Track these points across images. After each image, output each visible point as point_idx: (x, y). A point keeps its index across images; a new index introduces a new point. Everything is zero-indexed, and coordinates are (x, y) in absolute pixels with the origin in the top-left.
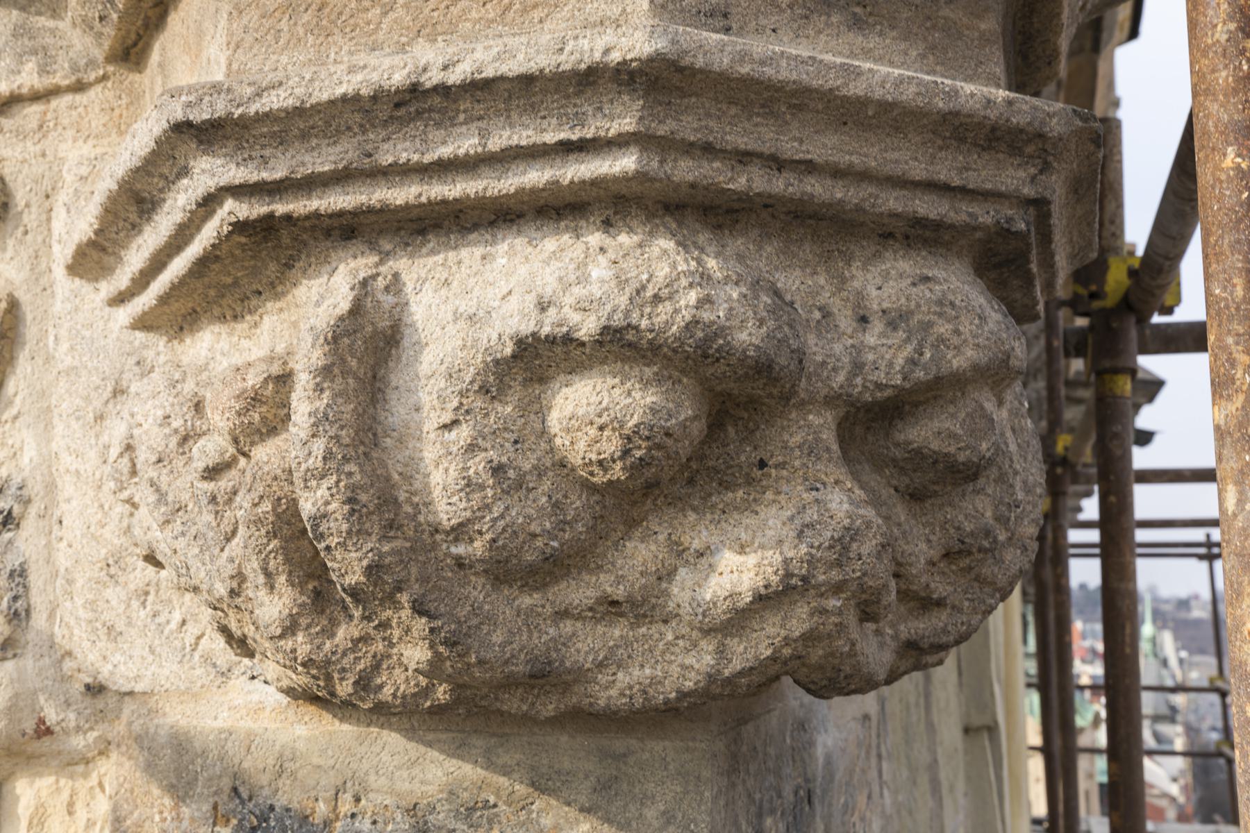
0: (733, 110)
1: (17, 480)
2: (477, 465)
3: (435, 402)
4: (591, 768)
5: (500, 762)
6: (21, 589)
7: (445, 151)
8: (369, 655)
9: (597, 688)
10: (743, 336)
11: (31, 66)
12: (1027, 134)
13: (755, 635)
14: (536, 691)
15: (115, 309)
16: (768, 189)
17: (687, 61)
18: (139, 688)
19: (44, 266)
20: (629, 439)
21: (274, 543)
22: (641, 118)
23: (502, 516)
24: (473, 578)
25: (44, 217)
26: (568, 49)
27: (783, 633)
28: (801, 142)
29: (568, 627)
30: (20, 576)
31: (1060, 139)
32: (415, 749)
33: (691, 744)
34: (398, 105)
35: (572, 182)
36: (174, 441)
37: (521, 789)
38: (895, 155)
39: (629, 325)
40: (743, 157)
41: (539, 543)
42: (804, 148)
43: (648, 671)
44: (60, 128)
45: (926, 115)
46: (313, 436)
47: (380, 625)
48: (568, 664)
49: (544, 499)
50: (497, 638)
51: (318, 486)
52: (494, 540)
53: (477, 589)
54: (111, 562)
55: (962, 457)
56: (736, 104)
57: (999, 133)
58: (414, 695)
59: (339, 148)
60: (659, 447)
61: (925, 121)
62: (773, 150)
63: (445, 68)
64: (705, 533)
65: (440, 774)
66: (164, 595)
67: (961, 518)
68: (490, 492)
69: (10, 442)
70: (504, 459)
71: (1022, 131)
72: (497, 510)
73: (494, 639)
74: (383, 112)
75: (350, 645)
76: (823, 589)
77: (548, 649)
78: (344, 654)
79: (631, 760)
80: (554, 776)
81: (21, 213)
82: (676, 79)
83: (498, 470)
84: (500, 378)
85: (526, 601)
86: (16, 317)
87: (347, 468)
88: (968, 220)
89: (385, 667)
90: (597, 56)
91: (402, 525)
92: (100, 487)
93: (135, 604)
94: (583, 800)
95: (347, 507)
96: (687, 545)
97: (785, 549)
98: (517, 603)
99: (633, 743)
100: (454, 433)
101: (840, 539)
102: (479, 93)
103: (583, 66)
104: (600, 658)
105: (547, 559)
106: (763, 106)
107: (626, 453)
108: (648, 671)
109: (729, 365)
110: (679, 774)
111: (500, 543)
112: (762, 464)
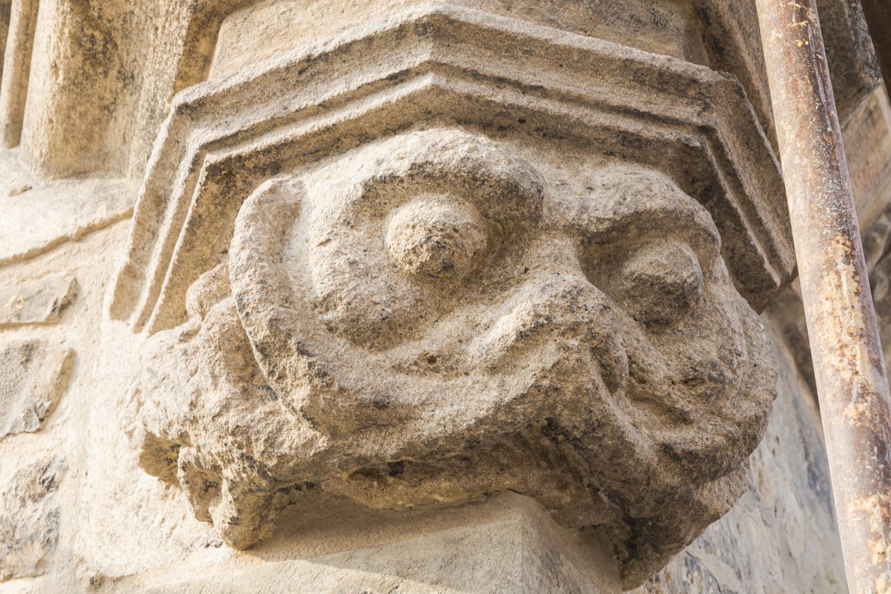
0: (489, 53)
1: (61, 457)
2: (341, 262)
3: (318, 233)
4: (439, 553)
5: (375, 564)
6: (54, 525)
7: (326, 96)
8: (275, 422)
9: (422, 422)
10: (499, 168)
11: (103, 207)
12: (685, 79)
13: (523, 371)
14: (383, 434)
15: (138, 334)
16: (516, 102)
17: (454, 17)
18: (127, 572)
19: (95, 327)
20: (430, 230)
21: (220, 354)
22: (432, 53)
23: (354, 289)
24: (338, 339)
25: (100, 297)
26: (390, 20)
27: (541, 365)
28: (535, 76)
29: (401, 378)
30: (55, 516)
31: (710, 85)
32: (316, 568)
33: (508, 522)
34: (300, 73)
35: (397, 101)
36: (165, 348)
37: (390, 579)
38: (599, 89)
39: (427, 162)
40: (500, 82)
41: (379, 308)
42: (537, 78)
43: (455, 407)
44: (116, 242)
45: (612, 61)
46: (242, 248)
47: (279, 378)
48: (401, 400)
49: (383, 283)
50: (353, 375)
51: (243, 278)
52: (349, 304)
53: (341, 345)
54: (118, 491)
55: (669, 280)
56: (490, 49)
57: (665, 78)
58: (304, 446)
59: (269, 108)
60: (450, 237)
61: (613, 67)
62: (516, 78)
63: (325, 44)
64: (490, 314)
65: (333, 581)
66: (151, 506)
67: (691, 351)
68: (347, 276)
69: (59, 436)
70: (357, 259)
71: (680, 76)
72: (352, 285)
73: (351, 376)
74: (293, 77)
75: (263, 416)
76: (563, 328)
77: (388, 388)
78: (259, 421)
79: (466, 542)
80: (413, 565)
81: (85, 299)
82: (450, 28)
83: (353, 263)
84: (357, 213)
85: (373, 358)
86: (73, 362)
87: (261, 264)
88: (657, 136)
89: (285, 429)
90: (405, 18)
91: (293, 302)
92: (116, 445)
93: (132, 513)
94: (433, 576)
95: (259, 286)
96: (478, 321)
97: (534, 299)
98: (367, 358)
99: (468, 529)
100: (327, 248)
101: (569, 292)
102: (344, 55)
103: (398, 25)
104: (424, 399)
105: (384, 319)
106: (507, 51)
107: (428, 239)
108: (455, 407)
109: (491, 186)
110: (500, 543)
111: (353, 305)
112: (526, 270)
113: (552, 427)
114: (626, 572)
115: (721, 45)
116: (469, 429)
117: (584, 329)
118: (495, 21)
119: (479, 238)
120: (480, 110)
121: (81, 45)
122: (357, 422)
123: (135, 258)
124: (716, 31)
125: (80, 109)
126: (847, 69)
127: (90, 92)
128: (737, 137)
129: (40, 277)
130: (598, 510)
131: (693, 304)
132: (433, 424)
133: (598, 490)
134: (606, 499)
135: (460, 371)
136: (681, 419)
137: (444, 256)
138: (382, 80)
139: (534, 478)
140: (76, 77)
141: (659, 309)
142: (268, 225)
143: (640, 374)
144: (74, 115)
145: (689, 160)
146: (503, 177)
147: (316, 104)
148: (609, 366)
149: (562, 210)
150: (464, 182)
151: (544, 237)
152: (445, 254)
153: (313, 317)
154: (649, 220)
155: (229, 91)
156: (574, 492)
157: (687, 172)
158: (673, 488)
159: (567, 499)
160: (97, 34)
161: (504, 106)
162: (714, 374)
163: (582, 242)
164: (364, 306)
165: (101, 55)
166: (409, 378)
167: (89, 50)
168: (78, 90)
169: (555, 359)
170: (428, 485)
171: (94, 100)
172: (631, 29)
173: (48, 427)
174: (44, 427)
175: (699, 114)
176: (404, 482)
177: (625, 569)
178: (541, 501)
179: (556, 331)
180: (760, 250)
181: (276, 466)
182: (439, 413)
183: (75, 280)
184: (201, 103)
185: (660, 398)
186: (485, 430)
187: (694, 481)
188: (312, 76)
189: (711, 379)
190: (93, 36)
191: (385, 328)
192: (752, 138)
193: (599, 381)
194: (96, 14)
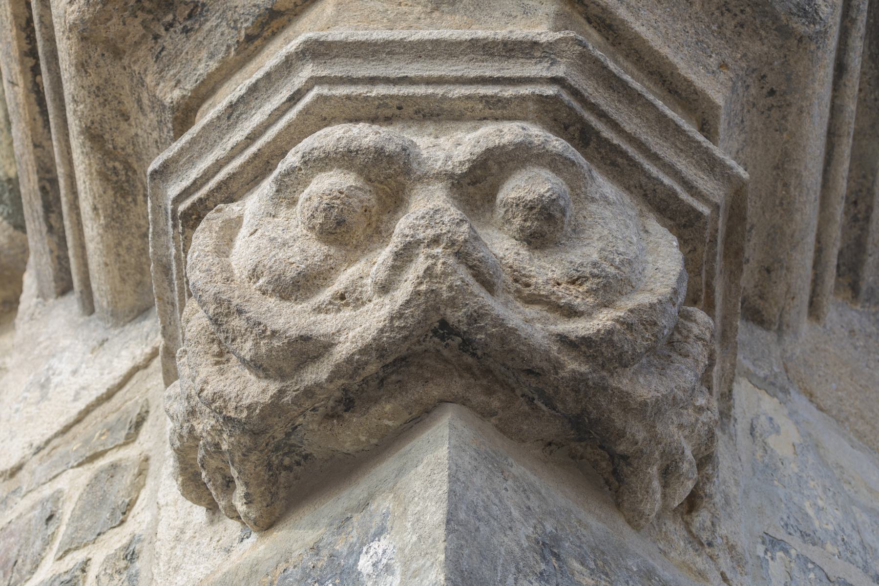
0: (359, 61)
23: (274, 256)
34: (229, 118)
40: (373, 81)
50: (282, 321)
71: (521, 42)
74: (224, 123)
82: (322, 49)
113: (444, 329)
114: (620, 500)
115: (608, 22)
116: (374, 340)
118: (358, 35)
119: (371, 200)
120: (363, 107)
121: (108, 180)
122: (294, 359)
123: (167, 337)
124: (596, 11)
125: (125, 243)
126: (773, 23)
127: (128, 224)
128: (597, 83)
129: (120, 408)
130: (538, 417)
131: (558, 215)
132: (348, 344)
133: (534, 399)
134: (544, 407)
135: (364, 299)
136: (571, 312)
137: (335, 214)
138: (284, 103)
139: (457, 386)
140: (113, 212)
141: (528, 224)
142: (214, 234)
143: (524, 279)
144: (122, 252)
145: (550, 109)
146: (371, 144)
147: (243, 138)
148: (475, 266)
149: (430, 162)
150: (343, 156)
151: (419, 186)
152: (335, 212)
153: (249, 287)
155: (182, 149)
156: (503, 398)
157: (555, 120)
158: (581, 374)
159: (495, 404)
160: (117, 164)
161: (379, 98)
162: (595, 271)
163: (453, 184)
164: (282, 267)
165: (126, 184)
166: (328, 317)
167: (116, 182)
168: (118, 225)
169: (425, 266)
170: (373, 410)
171: (133, 230)
172: (503, 23)
173: (129, 518)
174: (126, 518)
175: (548, 68)
176: (357, 415)
177: (618, 497)
178: (472, 408)
179: (422, 245)
180: (667, 181)
181: (248, 417)
182: (351, 335)
183: (147, 400)
184: (165, 166)
185: (547, 297)
186: (387, 337)
187: (603, 367)
188: (238, 117)
190: (115, 168)
192: (614, 82)
193: (470, 279)
194: (111, 146)
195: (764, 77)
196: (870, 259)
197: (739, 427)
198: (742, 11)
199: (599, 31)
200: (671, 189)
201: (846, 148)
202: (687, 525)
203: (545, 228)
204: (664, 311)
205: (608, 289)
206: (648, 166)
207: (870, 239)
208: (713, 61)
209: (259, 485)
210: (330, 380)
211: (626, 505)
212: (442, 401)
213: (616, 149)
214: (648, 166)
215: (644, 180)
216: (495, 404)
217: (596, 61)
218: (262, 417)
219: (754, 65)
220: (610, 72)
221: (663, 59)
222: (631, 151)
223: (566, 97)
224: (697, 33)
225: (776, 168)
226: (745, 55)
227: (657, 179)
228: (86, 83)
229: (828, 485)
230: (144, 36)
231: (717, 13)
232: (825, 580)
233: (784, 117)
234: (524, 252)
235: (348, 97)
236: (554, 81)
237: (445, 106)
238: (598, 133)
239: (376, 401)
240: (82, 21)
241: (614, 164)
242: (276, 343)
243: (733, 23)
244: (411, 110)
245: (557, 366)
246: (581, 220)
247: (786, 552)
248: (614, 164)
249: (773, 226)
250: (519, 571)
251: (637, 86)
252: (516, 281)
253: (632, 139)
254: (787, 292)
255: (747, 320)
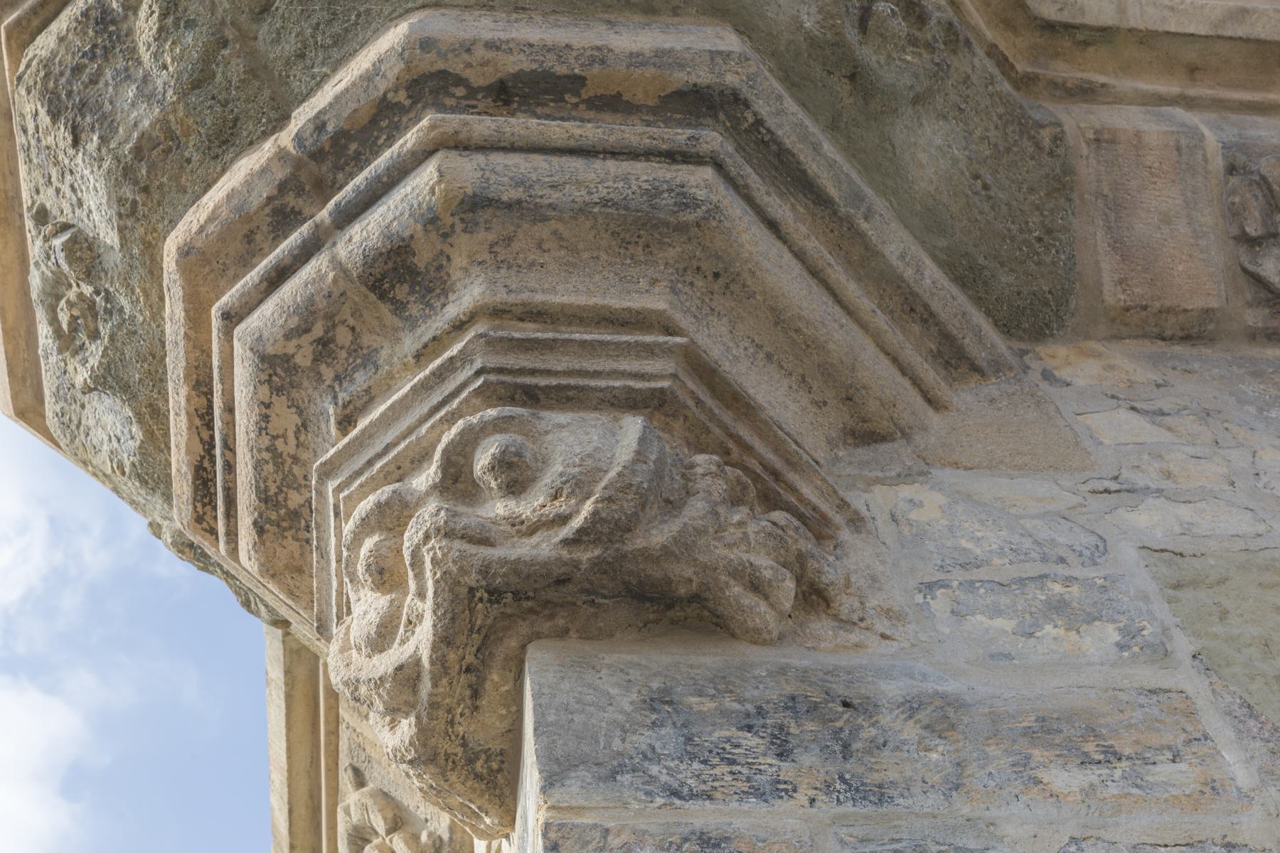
40: (370, 463)
74: (323, 562)
85: (391, 651)
117: (432, 531)
124: (519, 310)
131: (515, 459)
136: (563, 519)
139: (523, 628)
152: (373, 567)
154: (455, 448)
158: (598, 557)
178: (547, 637)
180: (617, 384)
189: (565, 483)
191: (383, 630)
195: (698, 268)
196: (967, 341)
197: (879, 523)
198: (639, 237)
199: (535, 321)
200: (625, 387)
201: (837, 274)
202: (836, 617)
203: (513, 475)
204: (634, 472)
205: (579, 486)
206: (593, 383)
207: (950, 327)
208: (643, 284)
209: (481, 796)
210: (435, 685)
211: (738, 631)
212: (523, 647)
213: (559, 388)
214: (593, 383)
215: (600, 395)
216: (561, 622)
217: (501, 339)
218: (424, 745)
219: (681, 266)
220: (518, 340)
221: (594, 308)
222: (572, 381)
223: (493, 378)
224: (616, 274)
225: (776, 324)
226: (667, 264)
227: (608, 387)
228: (304, 604)
229: (984, 518)
230: (301, 546)
231: (622, 251)
232: (996, 587)
233: (744, 286)
234: (512, 503)
235: (361, 486)
236: (479, 373)
237: (424, 444)
238: (536, 385)
239: (484, 679)
240: (262, 565)
241: (569, 399)
242: (388, 686)
243: (640, 249)
244: (407, 465)
245: (576, 564)
246: (544, 451)
247: (947, 586)
248: (569, 399)
249: (819, 366)
250: (625, 732)
251: (550, 335)
252: (513, 525)
253: (569, 373)
254: (882, 405)
255: (869, 444)
